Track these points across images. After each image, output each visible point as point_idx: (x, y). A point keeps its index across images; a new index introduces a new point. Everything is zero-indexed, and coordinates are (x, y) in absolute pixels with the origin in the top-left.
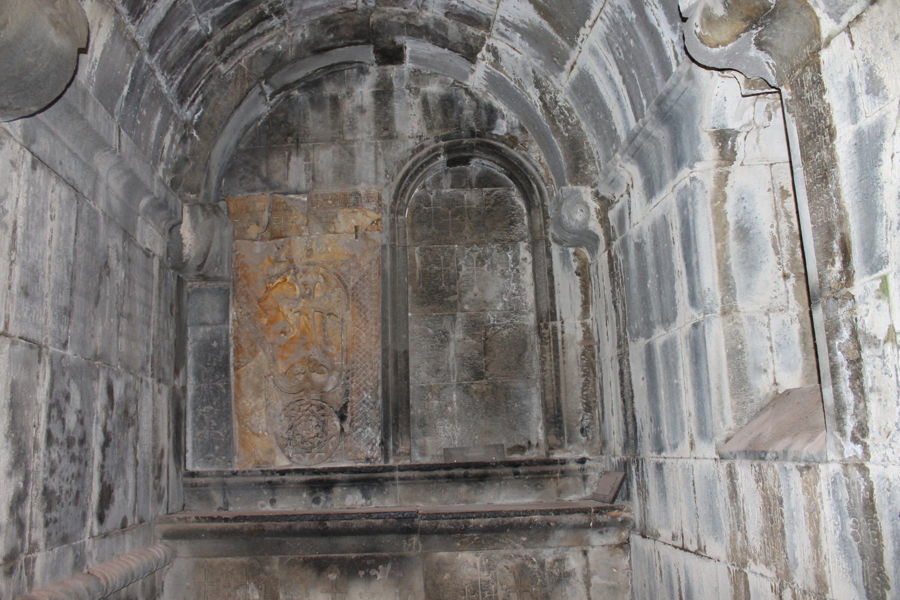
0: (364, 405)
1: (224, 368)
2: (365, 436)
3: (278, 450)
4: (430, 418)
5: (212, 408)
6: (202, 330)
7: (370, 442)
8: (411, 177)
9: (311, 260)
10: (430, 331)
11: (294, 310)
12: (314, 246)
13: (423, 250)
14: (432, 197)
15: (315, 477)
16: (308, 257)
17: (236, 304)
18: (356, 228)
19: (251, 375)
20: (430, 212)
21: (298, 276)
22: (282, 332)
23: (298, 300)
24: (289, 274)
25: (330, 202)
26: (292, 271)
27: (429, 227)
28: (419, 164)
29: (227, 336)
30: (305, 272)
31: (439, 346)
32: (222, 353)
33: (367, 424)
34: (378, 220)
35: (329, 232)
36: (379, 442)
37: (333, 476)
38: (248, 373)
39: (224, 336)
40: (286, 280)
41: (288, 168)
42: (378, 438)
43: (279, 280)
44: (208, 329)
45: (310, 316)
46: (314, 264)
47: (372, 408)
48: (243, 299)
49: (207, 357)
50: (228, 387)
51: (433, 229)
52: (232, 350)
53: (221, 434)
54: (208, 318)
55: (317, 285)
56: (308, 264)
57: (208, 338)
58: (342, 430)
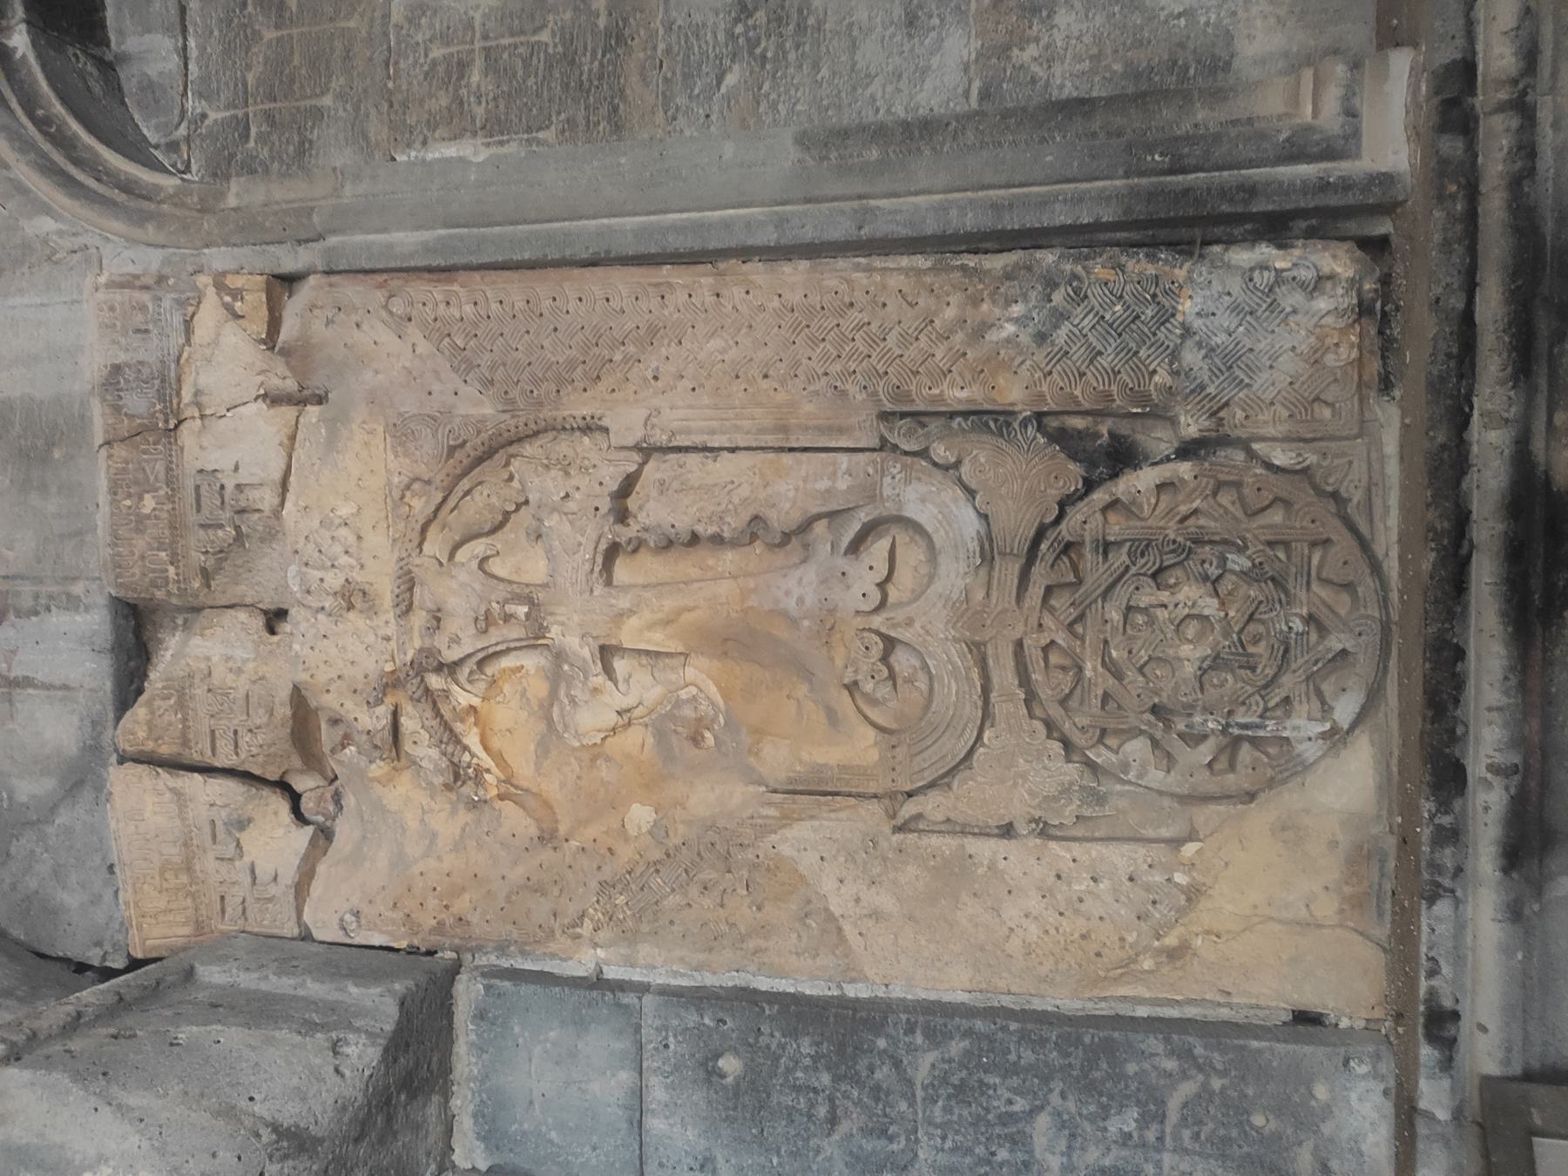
0: (1061, 335)
1: (846, 1030)
2: (1222, 329)
3: (1288, 799)
4: (1139, 44)
5: (1043, 1121)
6: (656, 1124)
7: (1267, 298)
8: (77, 162)
9: (386, 590)
10: (730, 79)
11: (600, 680)
12: (334, 580)
13: (403, 135)
14: (213, 116)
15: (1485, 574)
16: (372, 610)
17: (561, 943)
18: (274, 399)
19: (884, 900)
20: (269, 117)
21: (451, 655)
22: (696, 740)
23: (559, 656)
24: (446, 694)
25: (149, 503)
26: (435, 681)
27: (318, 114)
28: (32, 129)
29: (698, 998)
30: (437, 619)
31: (801, 28)
32: (772, 1037)
33: (1165, 316)
34: (220, 286)
35: (277, 512)
36: (1264, 251)
37: (1489, 477)
38: (876, 915)
39: (692, 1018)
40: (473, 709)
41: (27, 682)
42: (1242, 256)
43: (472, 739)
44: (657, 1092)
45: (624, 602)
46: (408, 582)
47: (1080, 297)
48: (540, 909)
49: (790, 1113)
50: (935, 1019)
51: (327, 101)
52: (763, 984)
53: (1187, 1089)
54: (609, 1088)
55: (495, 567)
56: (406, 608)
57: (699, 1096)
58: (1187, 451)
